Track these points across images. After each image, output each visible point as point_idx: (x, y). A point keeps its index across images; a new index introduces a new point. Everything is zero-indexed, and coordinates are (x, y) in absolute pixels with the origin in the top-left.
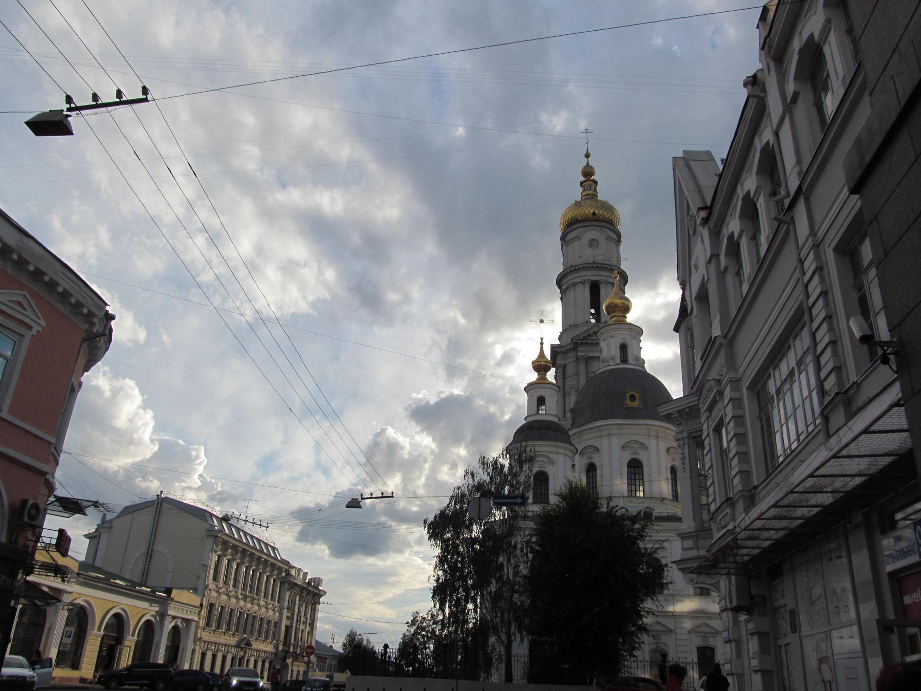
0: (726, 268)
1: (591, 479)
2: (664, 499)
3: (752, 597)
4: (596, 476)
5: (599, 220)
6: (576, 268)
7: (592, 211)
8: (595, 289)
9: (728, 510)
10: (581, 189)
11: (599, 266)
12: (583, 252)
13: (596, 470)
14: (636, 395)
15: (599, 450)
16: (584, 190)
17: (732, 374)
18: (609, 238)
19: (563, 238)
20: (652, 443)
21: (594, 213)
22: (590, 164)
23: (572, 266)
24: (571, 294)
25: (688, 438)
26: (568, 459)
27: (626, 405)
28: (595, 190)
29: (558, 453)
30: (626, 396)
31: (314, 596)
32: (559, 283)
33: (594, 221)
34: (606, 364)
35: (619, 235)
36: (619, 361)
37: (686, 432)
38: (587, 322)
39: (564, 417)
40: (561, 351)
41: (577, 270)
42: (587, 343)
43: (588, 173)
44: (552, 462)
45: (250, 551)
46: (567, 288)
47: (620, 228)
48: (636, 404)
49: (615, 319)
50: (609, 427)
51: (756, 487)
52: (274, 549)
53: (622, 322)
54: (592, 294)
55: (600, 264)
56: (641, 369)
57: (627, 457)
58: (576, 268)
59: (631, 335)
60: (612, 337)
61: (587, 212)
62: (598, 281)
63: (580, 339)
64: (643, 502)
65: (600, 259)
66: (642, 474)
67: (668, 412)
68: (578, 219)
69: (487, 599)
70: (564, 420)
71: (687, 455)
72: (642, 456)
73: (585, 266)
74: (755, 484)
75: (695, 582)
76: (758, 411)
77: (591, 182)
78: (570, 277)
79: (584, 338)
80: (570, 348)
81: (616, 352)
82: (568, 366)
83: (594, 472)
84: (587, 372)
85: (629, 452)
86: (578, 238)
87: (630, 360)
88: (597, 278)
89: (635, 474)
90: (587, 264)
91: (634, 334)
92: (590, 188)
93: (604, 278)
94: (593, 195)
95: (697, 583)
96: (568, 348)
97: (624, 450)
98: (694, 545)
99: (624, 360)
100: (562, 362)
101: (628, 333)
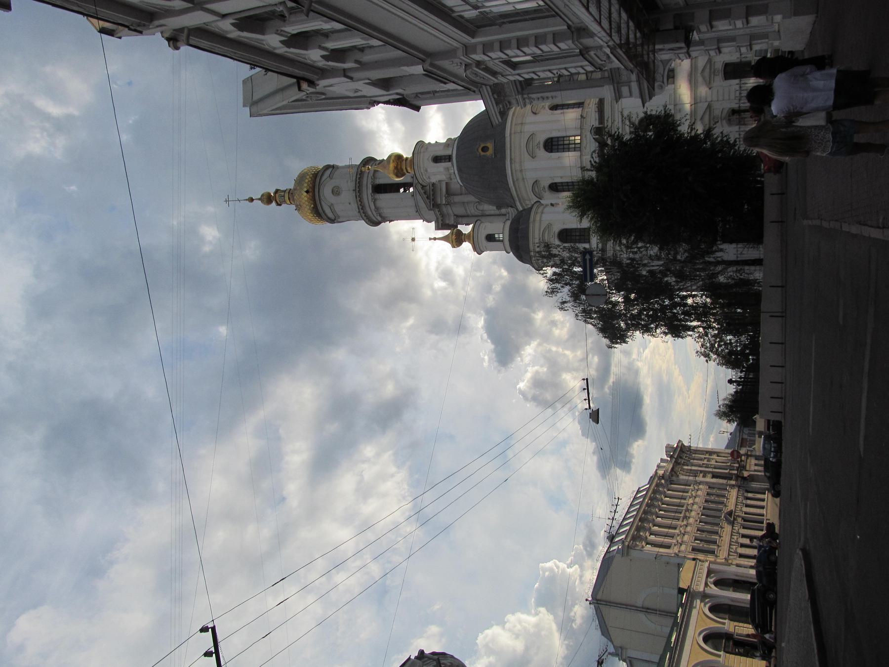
0: (357, 62)
1: (564, 187)
2: (582, 116)
3: (676, 28)
4: (562, 183)
5: (314, 187)
6: (360, 207)
7: (305, 194)
8: (380, 189)
9: (592, 53)
10: (283, 205)
11: (358, 185)
12: (345, 201)
13: (556, 183)
14: (482, 145)
15: (536, 181)
16: (285, 202)
17: (460, 53)
18: (331, 177)
19: (332, 221)
20: (528, 129)
21: (307, 192)
22: (260, 197)
23: (359, 212)
24: (386, 212)
25: (523, 94)
26: (546, 210)
27: (492, 155)
28: (285, 191)
29: (540, 220)
30: (484, 155)
31: (683, 452)
32: (376, 224)
33: (314, 191)
34: (453, 176)
35: (327, 167)
36: (450, 163)
37: (517, 97)
38: (413, 196)
39: (505, 215)
40: (442, 220)
41: (362, 207)
42: (433, 195)
43: (268, 199)
44: (549, 226)
45: (642, 515)
46: (381, 216)
48: (490, 145)
49: (409, 169)
50: (514, 171)
51: (569, 27)
52: (638, 491)
53: (411, 161)
54: (386, 192)
56: (457, 140)
57: (542, 153)
58: (360, 207)
59: (424, 152)
60: (426, 171)
61: (306, 199)
62: (372, 185)
63: (430, 202)
64: (586, 136)
65: (351, 185)
66: (558, 138)
67: (498, 114)
68: (313, 208)
69: (684, 285)
70: (508, 215)
71: (539, 95)
72: (542, 138)
73: (358, 199)
74: (566, 27)
75: (662, 84)
76: (493, 27)
77: (277, 195)
78: (370, 213)
79: (427, 198)
80: (439, 211)
81: (442, 166)
82: (456, 213)
83: (558, 184)
84: (461, 194)
85: (537, 150)
86: (331, 206)
87: (448, 152)
88: (370, 186)
89: (558, 145)
90: (356, 198)
91: (422, 150)
92: (283, 196)
93: (370, 181)
94: (289, 193)
95: (663, 82)
96: (438, 214)
97: (535, 157)
98: (626, 86)
99: (449, 158)
100: (452, 219)
101: (422, 155)
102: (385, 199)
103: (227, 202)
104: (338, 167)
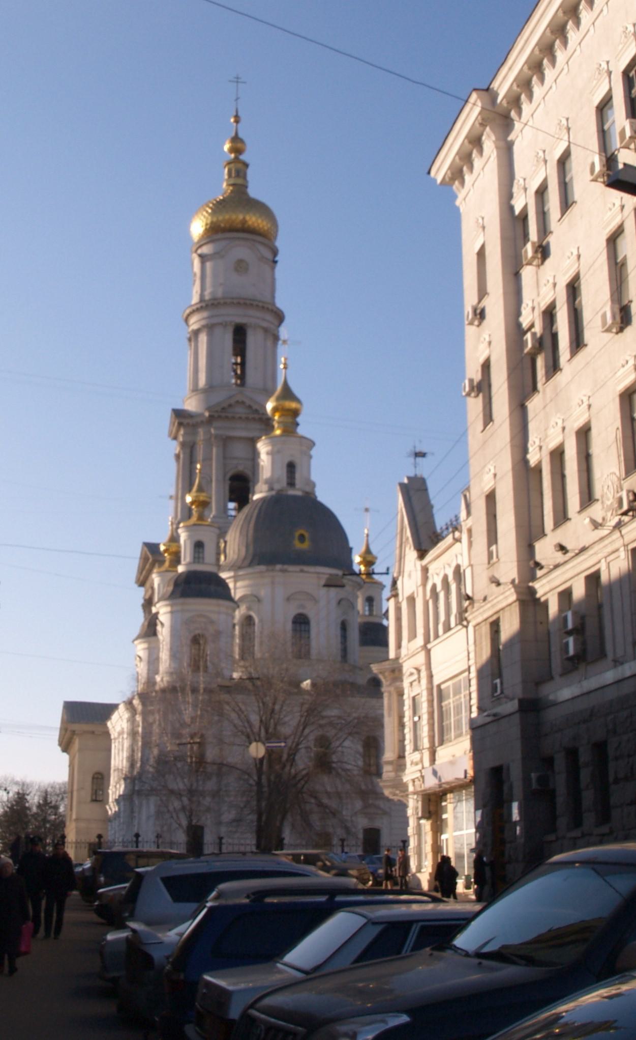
8: (240, 334)
14: (307, 535)
18: (262, 258)
22: (241, 135)
35: (275, 252)
42: (227, 417)
47: (279, 243)
48: (306, 546)
54: (235, 341)
55: (250, 300)
57: (293, 611)
62: (245, 325)
63: (217, 411)
66: (309, 631)
79: (223, 409)
99: (291, 483)
102: (228, 339)
103: (236, 80)
104: (273, 269)
